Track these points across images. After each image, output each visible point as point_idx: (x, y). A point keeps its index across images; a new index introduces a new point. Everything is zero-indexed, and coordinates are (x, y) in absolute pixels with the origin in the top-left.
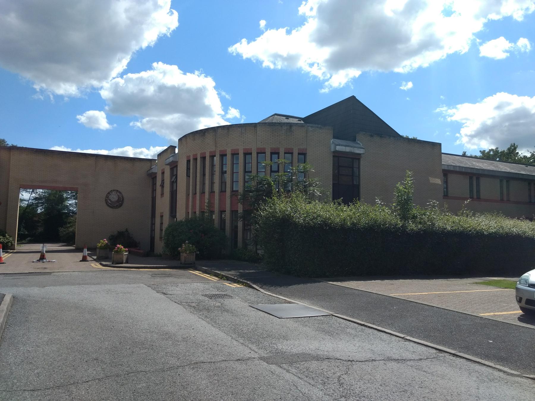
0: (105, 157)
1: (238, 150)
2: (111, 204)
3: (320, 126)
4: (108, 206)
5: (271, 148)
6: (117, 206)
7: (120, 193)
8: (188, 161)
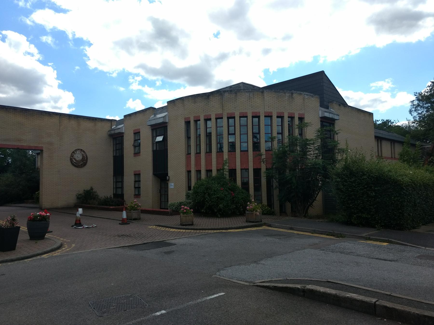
0: (68, 116)
1: (234, 113)
2: (76, 163)
3: (312, 94)
4: (73, 164)
5: (277, 112)
6: (82, 165)
7: (84, 151)
8: (188, 123)
